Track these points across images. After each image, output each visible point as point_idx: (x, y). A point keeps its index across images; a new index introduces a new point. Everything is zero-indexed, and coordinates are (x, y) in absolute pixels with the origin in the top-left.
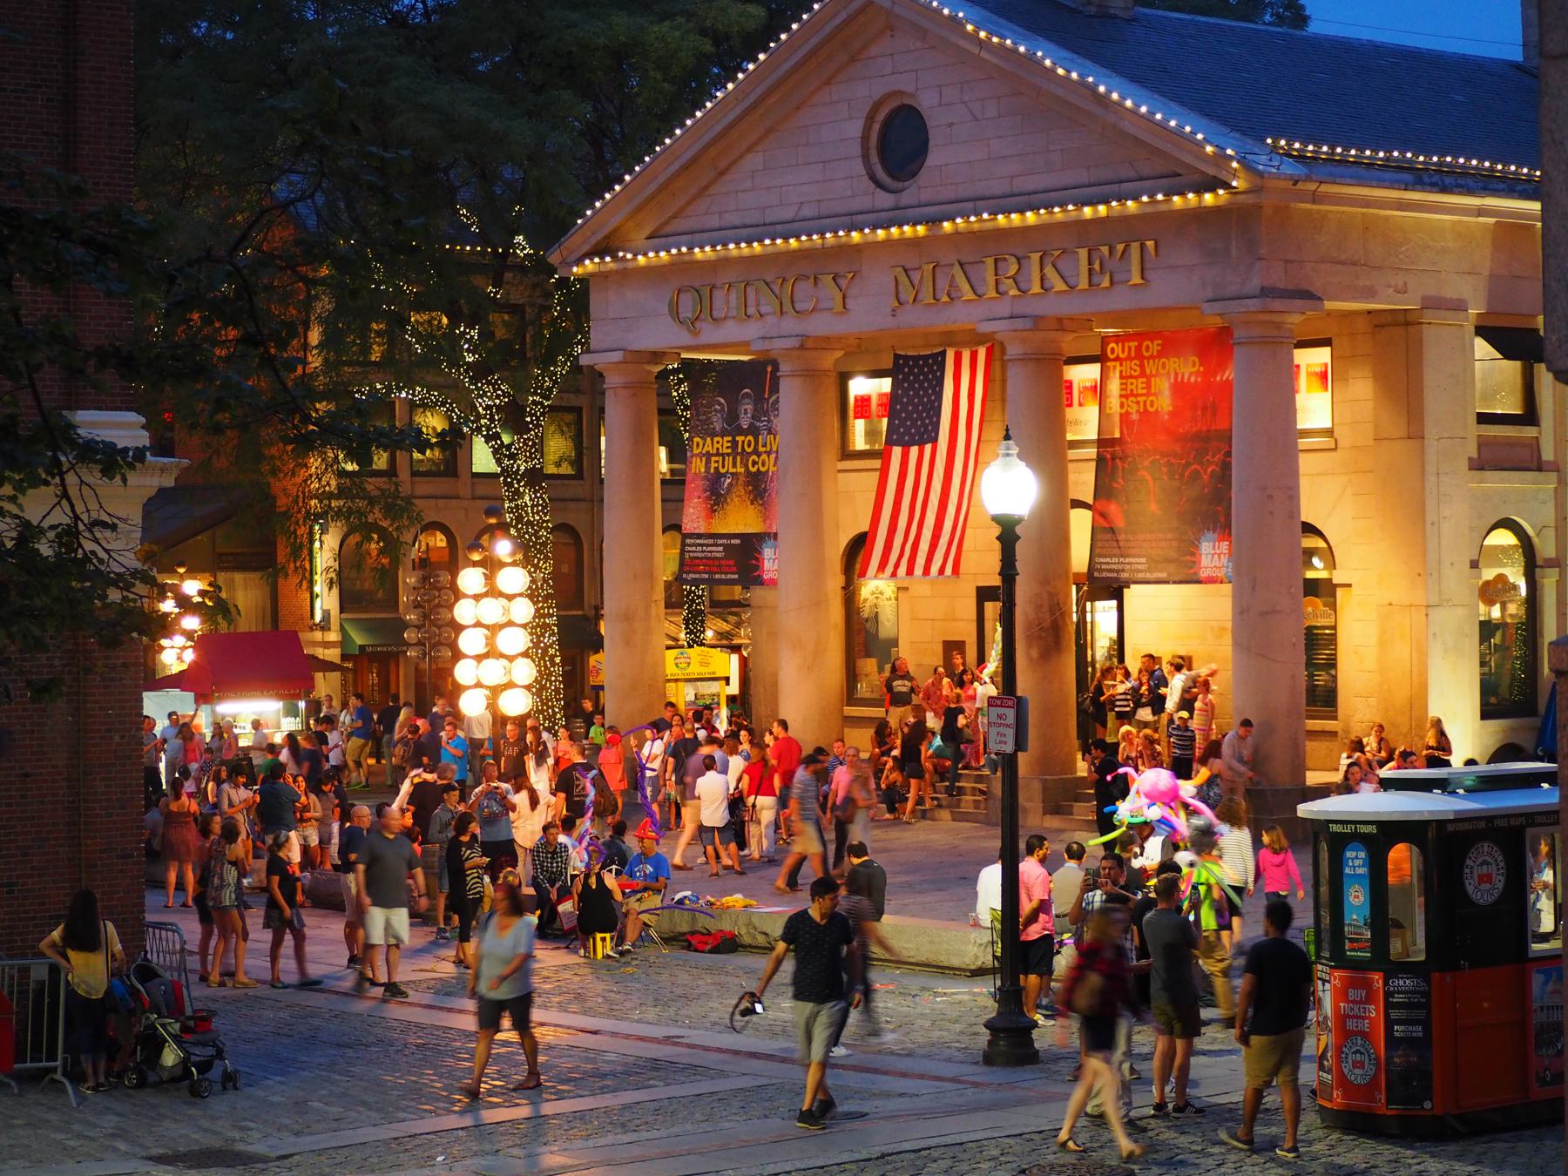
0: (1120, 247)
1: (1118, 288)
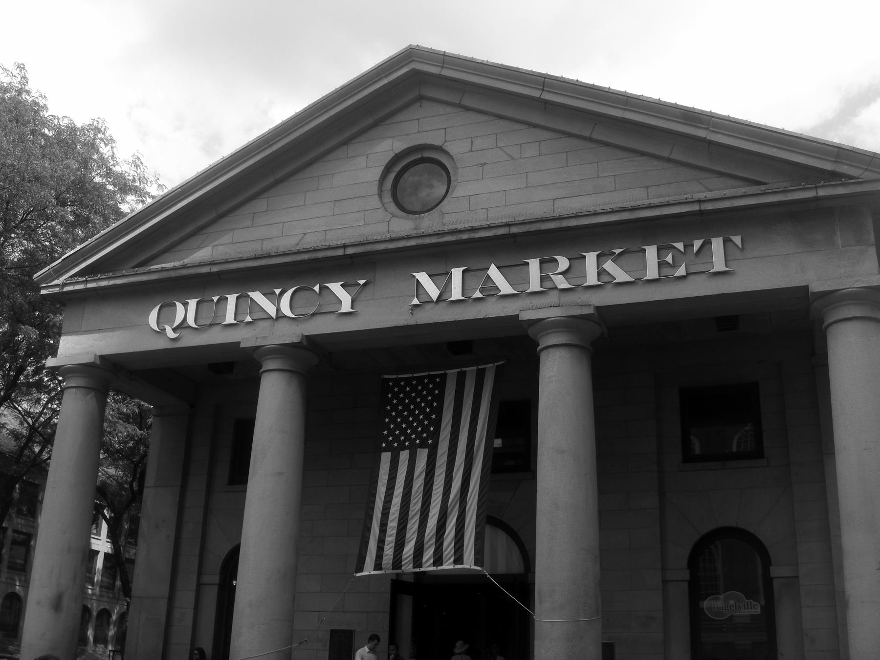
0: (697, 244)
1: (692, 278)
